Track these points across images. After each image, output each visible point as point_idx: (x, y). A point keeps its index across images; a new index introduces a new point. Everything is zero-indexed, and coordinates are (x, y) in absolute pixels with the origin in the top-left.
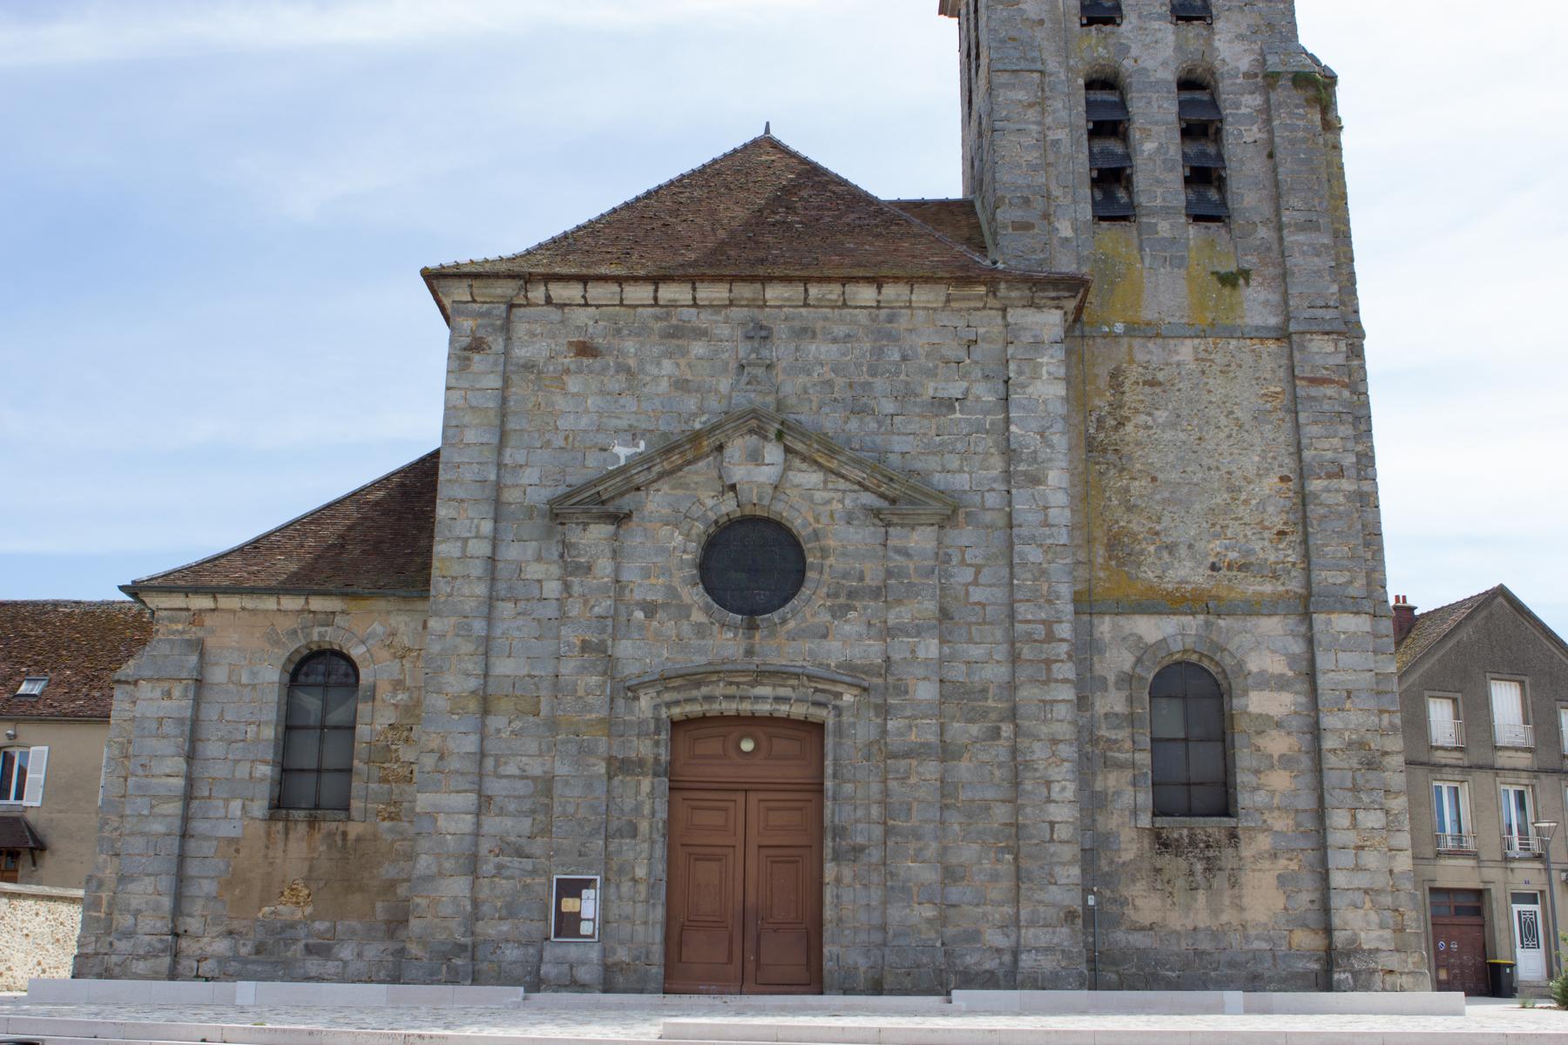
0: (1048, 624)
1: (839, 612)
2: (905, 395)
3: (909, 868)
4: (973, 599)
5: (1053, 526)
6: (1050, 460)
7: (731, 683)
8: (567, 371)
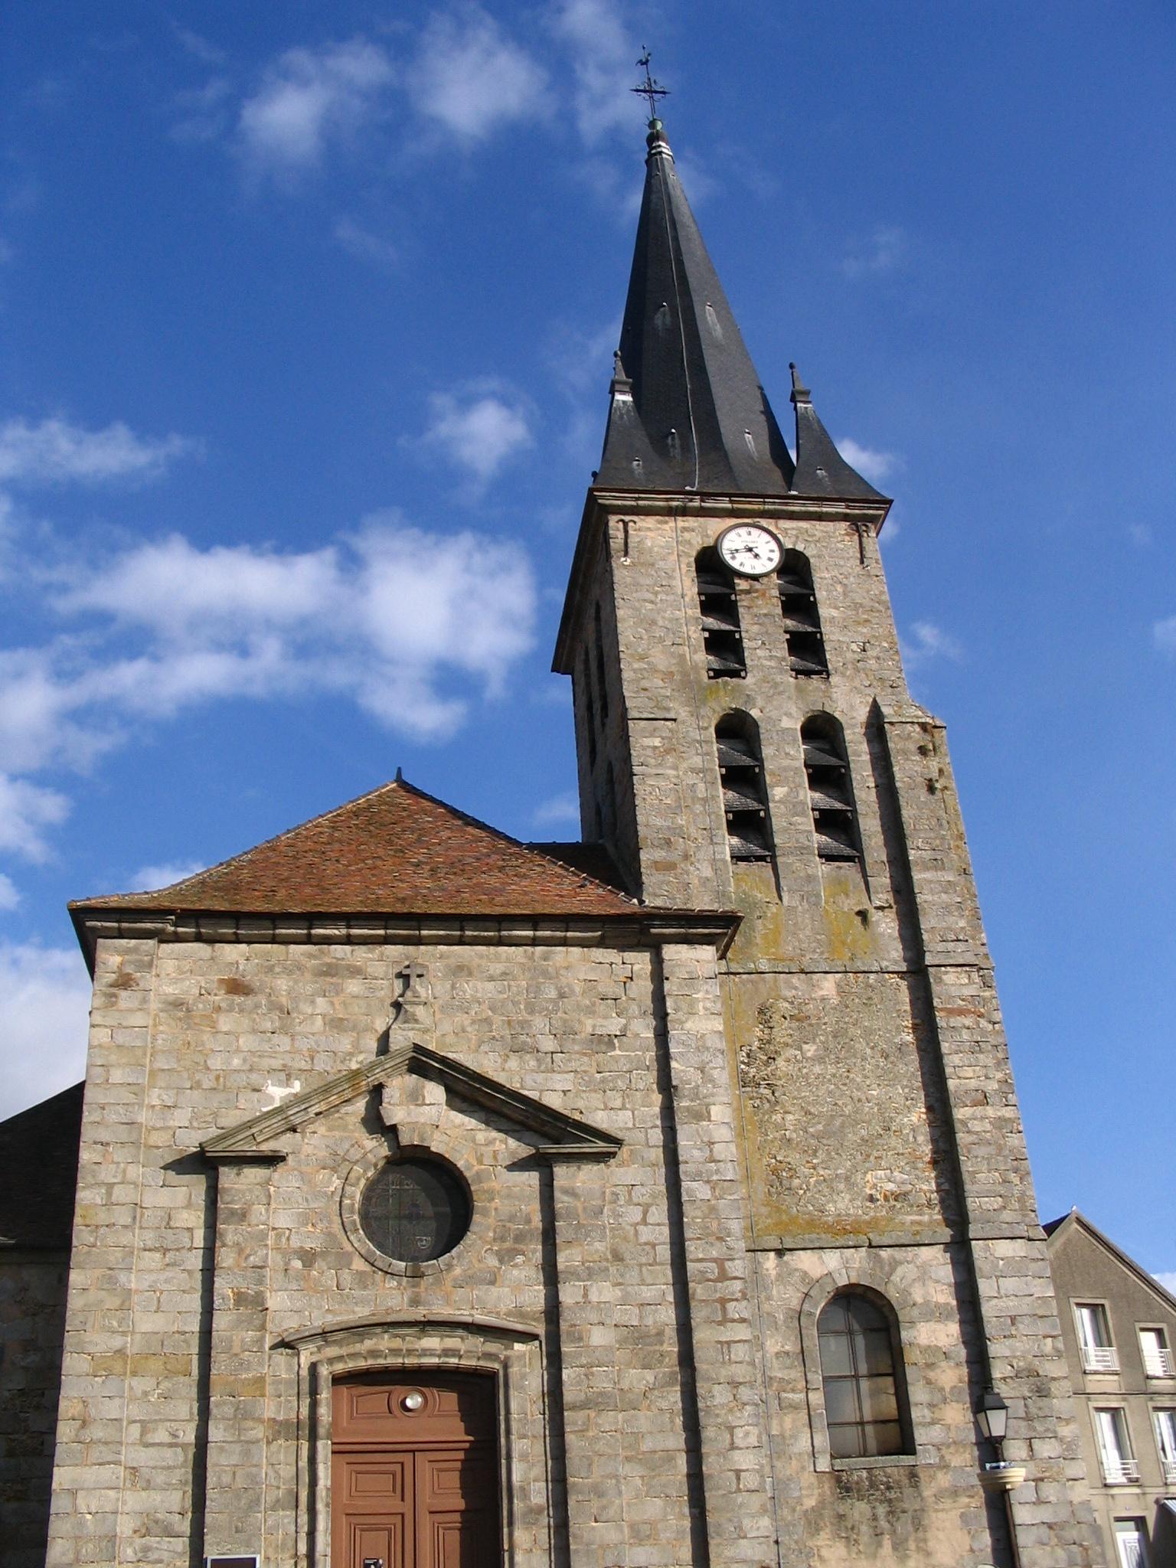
0: (720, 1262)
1: (506, 1257)
2: (565, 1033)
3: (593, 1528)
4: (643, 1240)
5: (719, 1161)
6: (712, 1095)
7: (397, 1336)
8: (218, 1009)
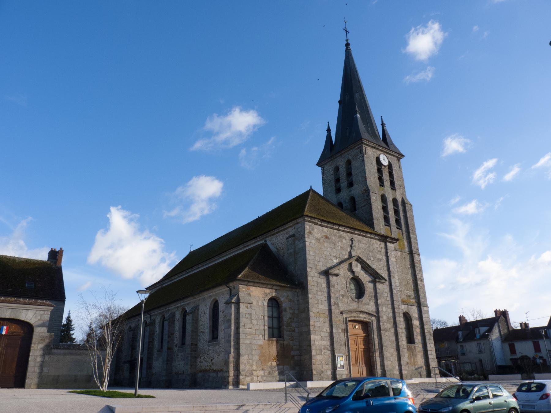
1: (370, 300)
